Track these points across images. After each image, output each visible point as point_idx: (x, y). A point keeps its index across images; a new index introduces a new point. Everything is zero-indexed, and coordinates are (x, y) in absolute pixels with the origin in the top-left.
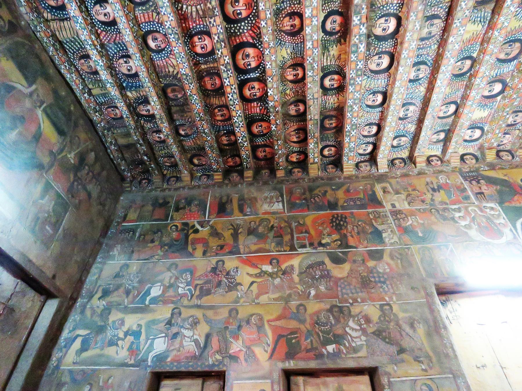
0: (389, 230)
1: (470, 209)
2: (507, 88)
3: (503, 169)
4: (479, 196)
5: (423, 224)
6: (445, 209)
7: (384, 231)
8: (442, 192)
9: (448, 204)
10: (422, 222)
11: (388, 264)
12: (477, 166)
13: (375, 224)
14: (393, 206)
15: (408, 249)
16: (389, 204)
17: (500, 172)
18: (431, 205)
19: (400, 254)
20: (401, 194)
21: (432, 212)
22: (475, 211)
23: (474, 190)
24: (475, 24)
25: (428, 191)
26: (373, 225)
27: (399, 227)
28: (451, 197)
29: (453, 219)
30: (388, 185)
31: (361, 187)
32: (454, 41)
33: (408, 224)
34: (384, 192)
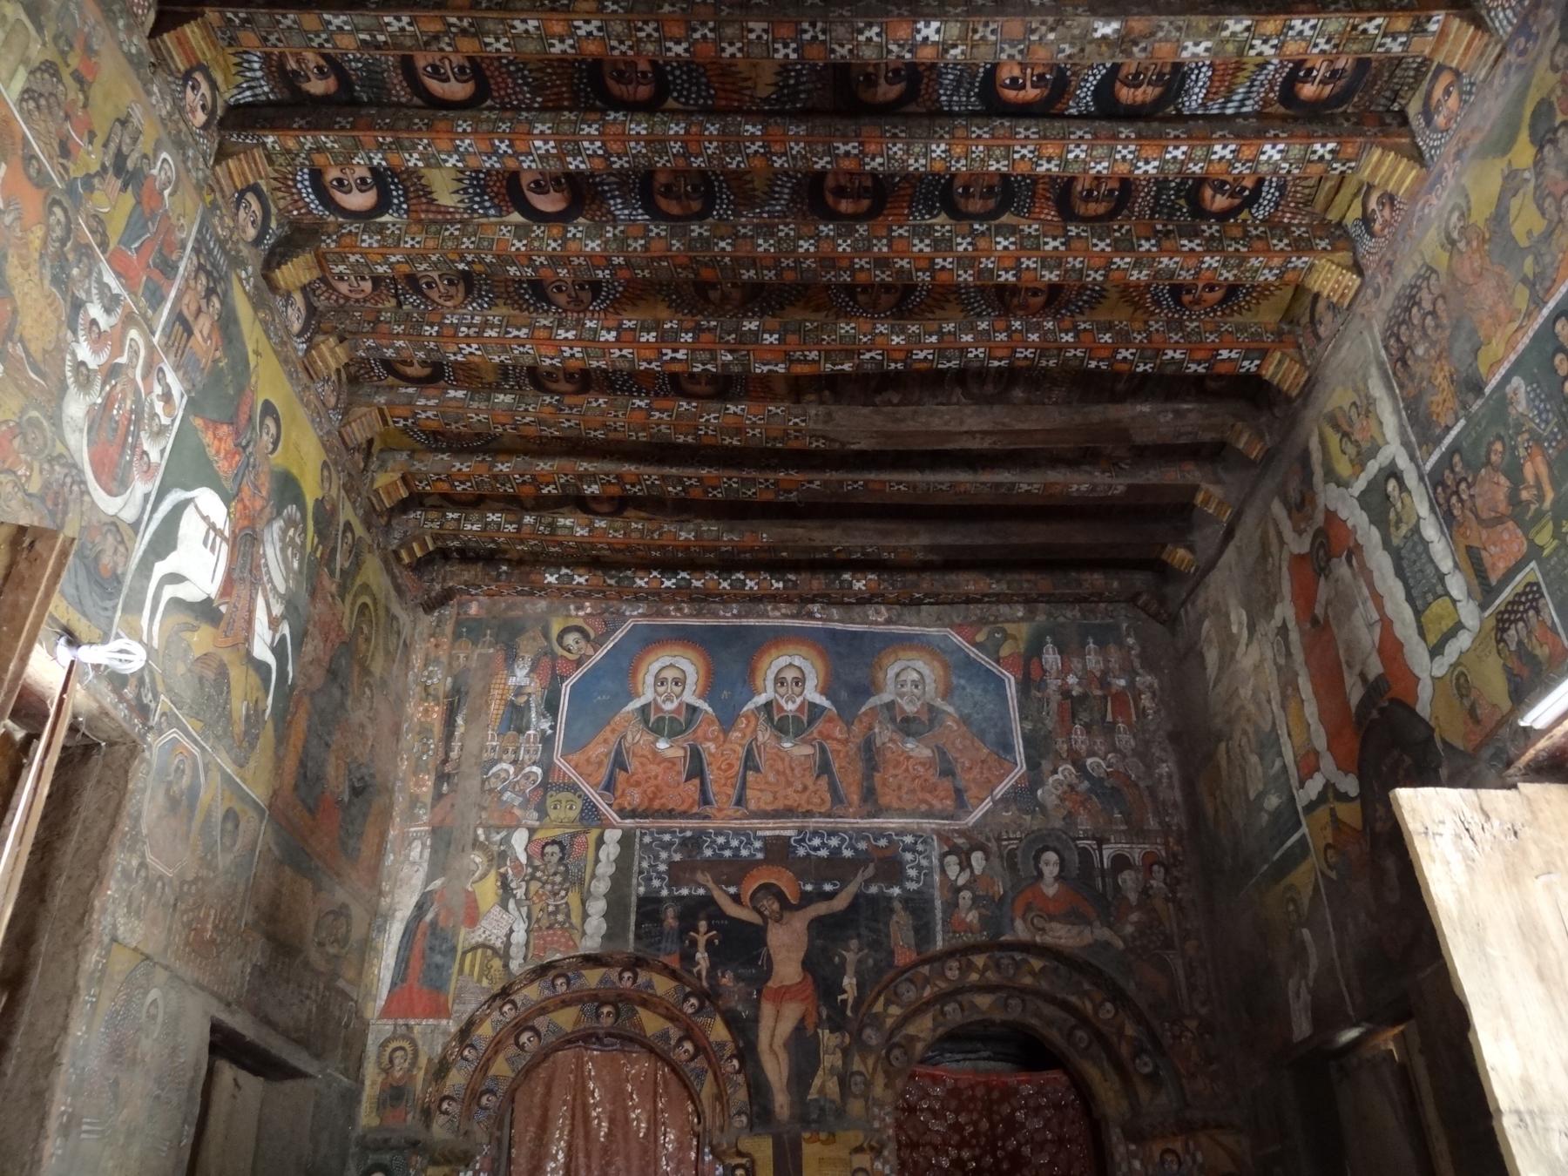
2: (556, 231)
3: (266, 331)
4: (178, 327)
8: (129, 199)
9: (103, 245)
12: (245, 252)
17: (258, 328)
18: (71, 190)
20: (40, 28)
21: (51, 213)
22: (137, 353)
23: (186, 300)
24: (778, 74)
25: (105, 145)
28: (127, 244)
29: (77, 306)
32: (752, 36)
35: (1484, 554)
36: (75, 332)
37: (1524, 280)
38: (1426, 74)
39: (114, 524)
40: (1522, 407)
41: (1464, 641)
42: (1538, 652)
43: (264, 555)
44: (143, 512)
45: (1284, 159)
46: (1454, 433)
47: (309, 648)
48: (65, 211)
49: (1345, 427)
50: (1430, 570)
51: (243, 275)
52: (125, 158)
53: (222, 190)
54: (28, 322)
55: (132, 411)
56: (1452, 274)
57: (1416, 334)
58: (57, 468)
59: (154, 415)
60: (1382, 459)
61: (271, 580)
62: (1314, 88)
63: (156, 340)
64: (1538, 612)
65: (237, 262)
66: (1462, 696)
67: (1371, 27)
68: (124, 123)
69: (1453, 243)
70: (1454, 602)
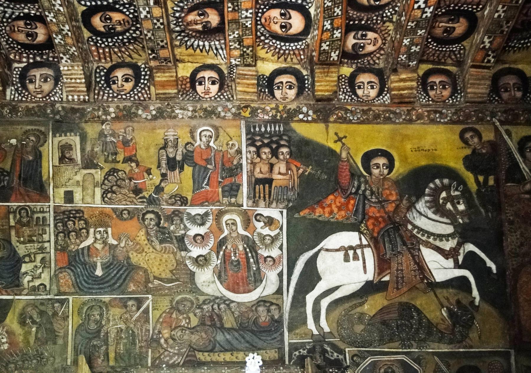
0: (39, 257)
1: (226, 217)
5: (116, 246)
6: (170, 219)
7: (27, 259)
10: (115, 243)
11: (10, 333)
12: (293, 106)
13: (14, 239)
14: (69, 197)
15: (62, 302)
16: (61, 191)
19: (42, 313)
26: (10, 242)
27: (61, 249)
30: (77, 139)
31: (14, 141)
33: (82, 246)
34: (62, 159)
36: (186, 250)
39: (262, 301)
43: (415, 227)
44: (281, 281)
47: (511, 240)
48: (152, 212)
51: (301, 116)
52: (175, 158)
53: (253, 101)
54: (155, 269)
55: (245, 249)
58: (205, 307)
59: (263, 238)
61: (430, 234)
63: (245, 207)
65: (292, 115)
68: (165, 147)
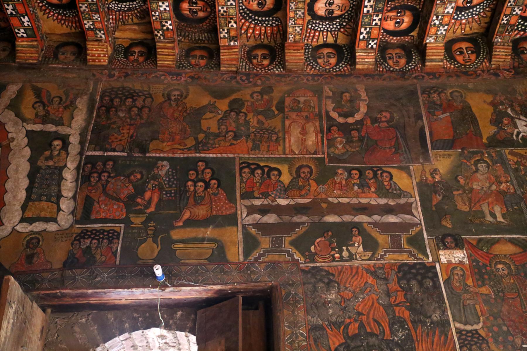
35: (96, 205)
37: (196, 139)
38: (197, 43)
40: (163, 172)
41: (52, 227)
42: (98, 257)
45: (161, 12)
46: (116, 154)
49: (45, 101)
50: (54, 189)
56: (161, 106)
57: (123, 108)
60: (63, 130)
62: (187, 7)
64: (110, 242)
66: (28, 246)
67: (233, 23)
69: (170, 99)
70: (59, 209)
